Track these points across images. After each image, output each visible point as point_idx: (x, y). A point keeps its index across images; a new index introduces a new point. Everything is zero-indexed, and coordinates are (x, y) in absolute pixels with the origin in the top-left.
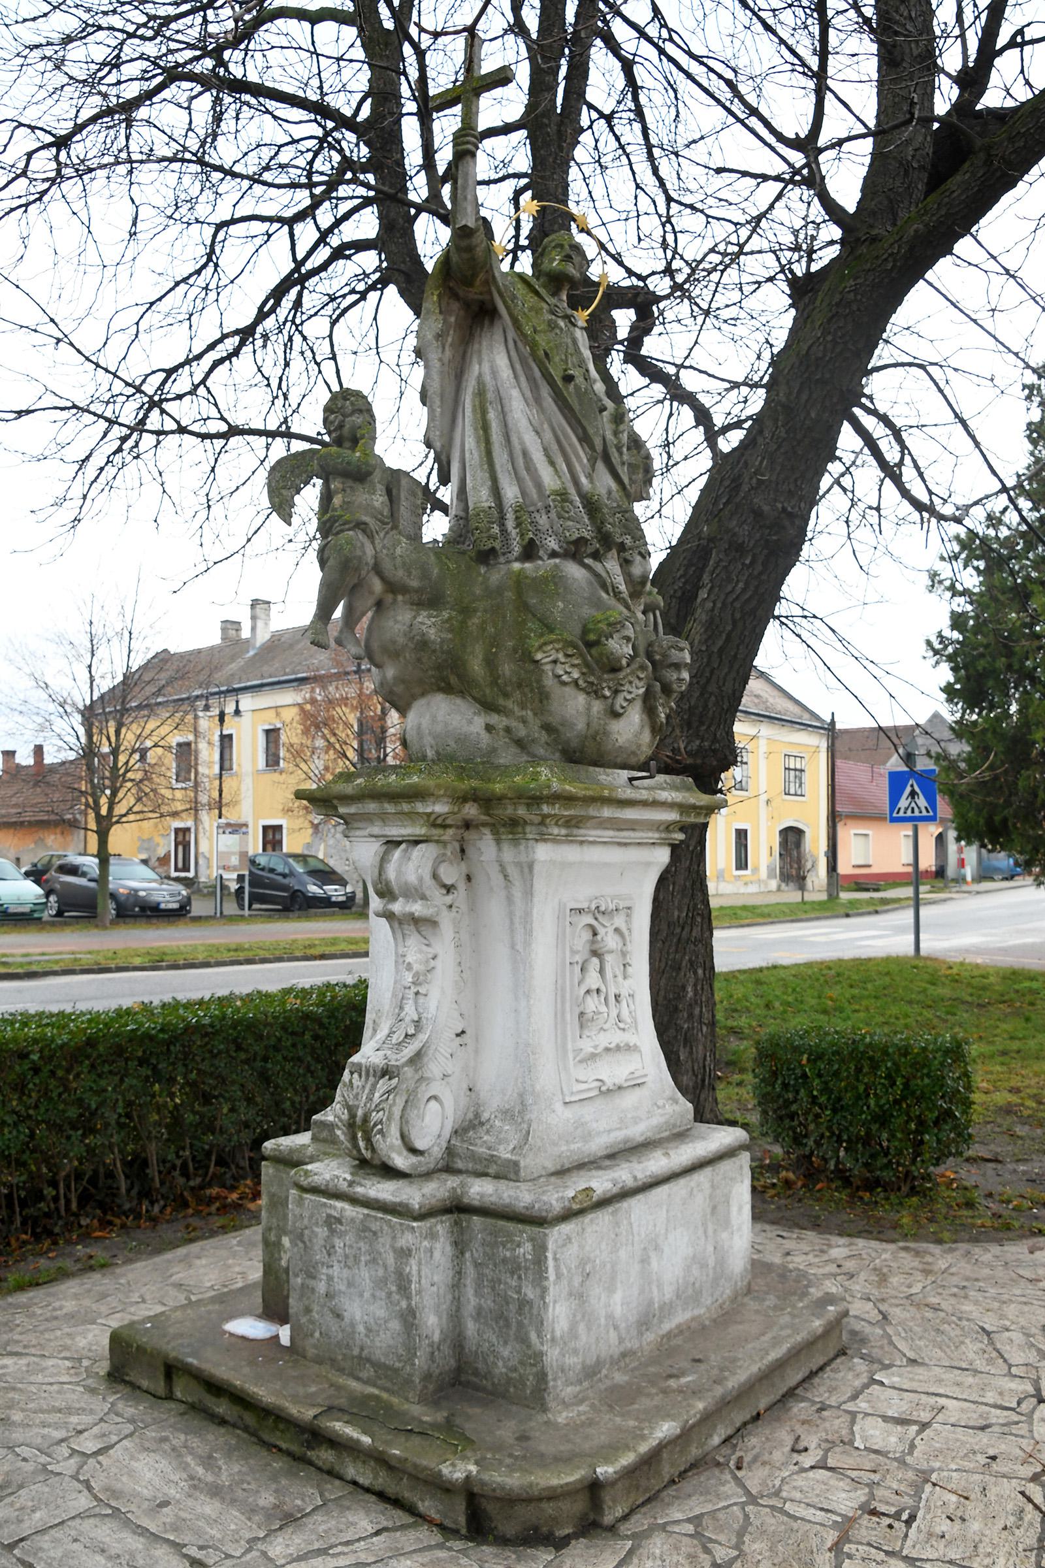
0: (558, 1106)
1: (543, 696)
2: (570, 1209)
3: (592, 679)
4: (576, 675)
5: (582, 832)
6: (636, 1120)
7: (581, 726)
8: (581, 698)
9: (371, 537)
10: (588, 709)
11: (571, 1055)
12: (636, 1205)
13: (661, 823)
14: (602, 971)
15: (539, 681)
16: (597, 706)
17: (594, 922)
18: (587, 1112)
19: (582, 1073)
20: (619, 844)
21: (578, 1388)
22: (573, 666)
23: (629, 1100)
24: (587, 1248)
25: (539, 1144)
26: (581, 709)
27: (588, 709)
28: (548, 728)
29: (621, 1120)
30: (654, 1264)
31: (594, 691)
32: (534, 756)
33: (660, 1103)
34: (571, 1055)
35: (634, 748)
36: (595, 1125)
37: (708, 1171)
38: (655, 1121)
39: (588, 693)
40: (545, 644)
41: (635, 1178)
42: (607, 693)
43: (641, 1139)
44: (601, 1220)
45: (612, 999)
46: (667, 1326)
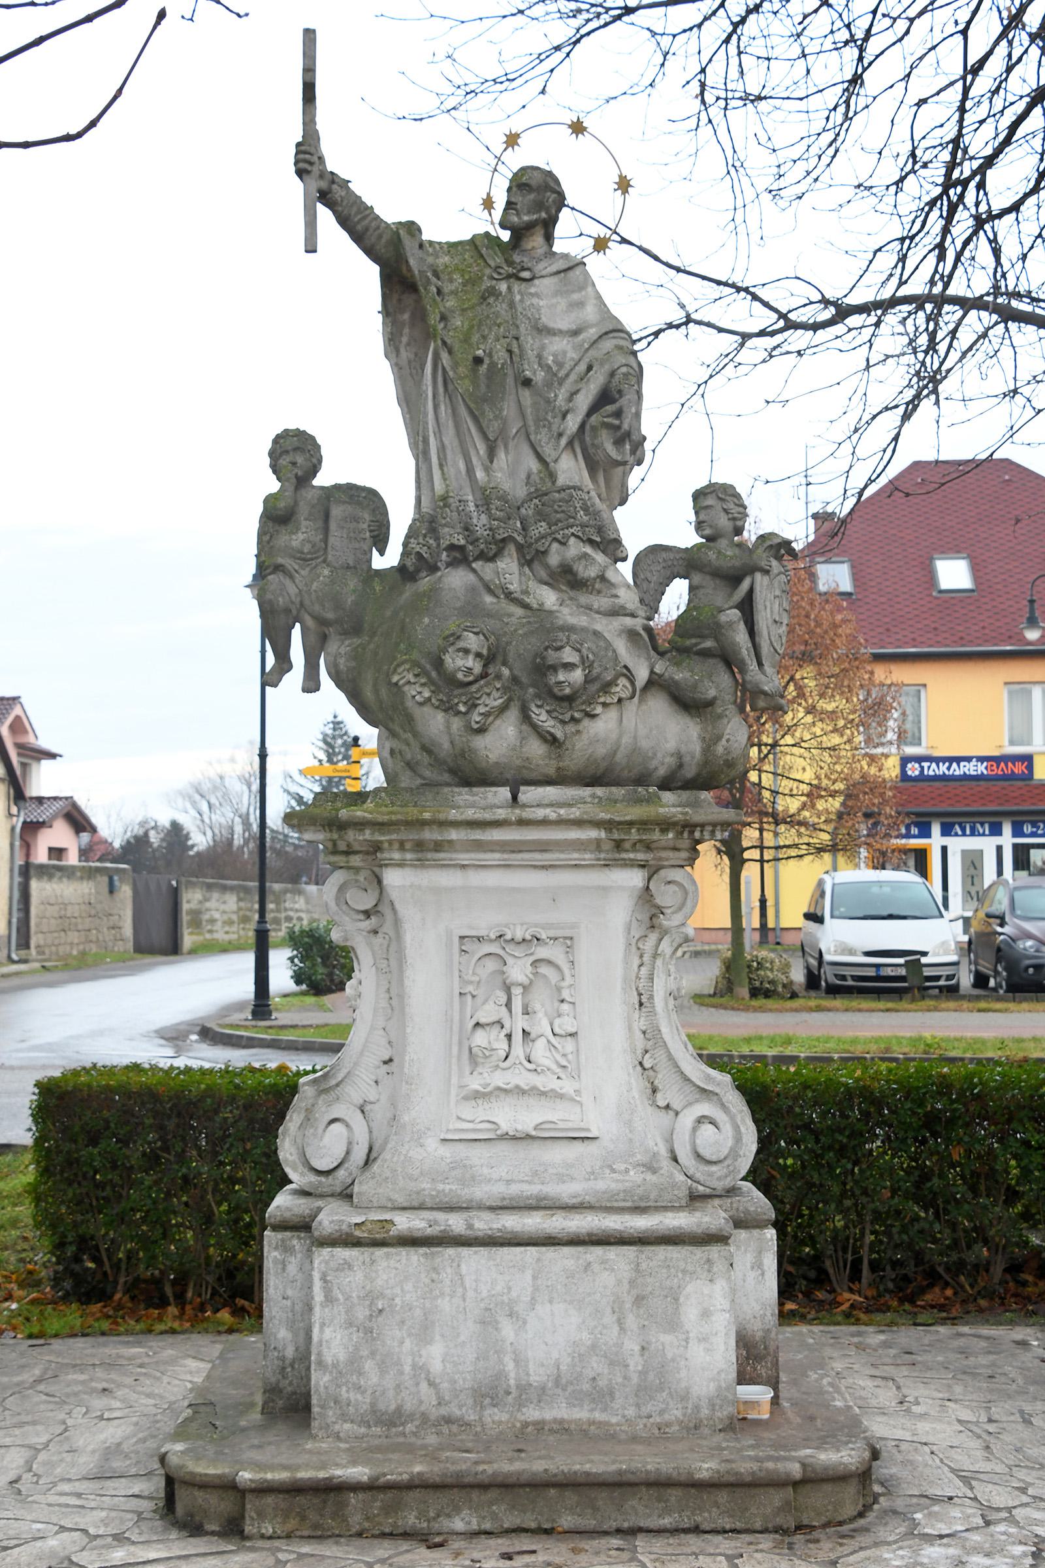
0: (432, 1144)
1: (409, 719)
2: (351, 1235)
3: (441, 696)
4: (427, 694)
5: (442, 855)
6: (561, 1179)
7: (446, 745)
8: (440, 716)
9: (291, 577)
10: (448, 727)
11: (454, 1091)
12: (473, 1260)
13: (590, 841)
14: (508, 1005)
15: (402, 703)
16: (457, 723)
17: (501, 952)
18: (478, 1156)
19: (468, 1111)
20: (535, 867)
21: (363, 1430)
22: (423, 685)
24: (379, 1282)
25: (388, 1174)
26: (441, 727)
27: (448, 727)
28: (424, 748)
29: (536, 1173)
30: (508, 1330)
31: (448, 708)
32: (424, 779)
34: (454, 1091)
35: (518, 762)
36: (486, 1171)
37: (630, 1251)
38: (601, 1185)
39: (445, 711)
40: (398, 666)
41: (470, 1227)
42: (462, 708)
45: (518, 1037)
46: (532, 1413)
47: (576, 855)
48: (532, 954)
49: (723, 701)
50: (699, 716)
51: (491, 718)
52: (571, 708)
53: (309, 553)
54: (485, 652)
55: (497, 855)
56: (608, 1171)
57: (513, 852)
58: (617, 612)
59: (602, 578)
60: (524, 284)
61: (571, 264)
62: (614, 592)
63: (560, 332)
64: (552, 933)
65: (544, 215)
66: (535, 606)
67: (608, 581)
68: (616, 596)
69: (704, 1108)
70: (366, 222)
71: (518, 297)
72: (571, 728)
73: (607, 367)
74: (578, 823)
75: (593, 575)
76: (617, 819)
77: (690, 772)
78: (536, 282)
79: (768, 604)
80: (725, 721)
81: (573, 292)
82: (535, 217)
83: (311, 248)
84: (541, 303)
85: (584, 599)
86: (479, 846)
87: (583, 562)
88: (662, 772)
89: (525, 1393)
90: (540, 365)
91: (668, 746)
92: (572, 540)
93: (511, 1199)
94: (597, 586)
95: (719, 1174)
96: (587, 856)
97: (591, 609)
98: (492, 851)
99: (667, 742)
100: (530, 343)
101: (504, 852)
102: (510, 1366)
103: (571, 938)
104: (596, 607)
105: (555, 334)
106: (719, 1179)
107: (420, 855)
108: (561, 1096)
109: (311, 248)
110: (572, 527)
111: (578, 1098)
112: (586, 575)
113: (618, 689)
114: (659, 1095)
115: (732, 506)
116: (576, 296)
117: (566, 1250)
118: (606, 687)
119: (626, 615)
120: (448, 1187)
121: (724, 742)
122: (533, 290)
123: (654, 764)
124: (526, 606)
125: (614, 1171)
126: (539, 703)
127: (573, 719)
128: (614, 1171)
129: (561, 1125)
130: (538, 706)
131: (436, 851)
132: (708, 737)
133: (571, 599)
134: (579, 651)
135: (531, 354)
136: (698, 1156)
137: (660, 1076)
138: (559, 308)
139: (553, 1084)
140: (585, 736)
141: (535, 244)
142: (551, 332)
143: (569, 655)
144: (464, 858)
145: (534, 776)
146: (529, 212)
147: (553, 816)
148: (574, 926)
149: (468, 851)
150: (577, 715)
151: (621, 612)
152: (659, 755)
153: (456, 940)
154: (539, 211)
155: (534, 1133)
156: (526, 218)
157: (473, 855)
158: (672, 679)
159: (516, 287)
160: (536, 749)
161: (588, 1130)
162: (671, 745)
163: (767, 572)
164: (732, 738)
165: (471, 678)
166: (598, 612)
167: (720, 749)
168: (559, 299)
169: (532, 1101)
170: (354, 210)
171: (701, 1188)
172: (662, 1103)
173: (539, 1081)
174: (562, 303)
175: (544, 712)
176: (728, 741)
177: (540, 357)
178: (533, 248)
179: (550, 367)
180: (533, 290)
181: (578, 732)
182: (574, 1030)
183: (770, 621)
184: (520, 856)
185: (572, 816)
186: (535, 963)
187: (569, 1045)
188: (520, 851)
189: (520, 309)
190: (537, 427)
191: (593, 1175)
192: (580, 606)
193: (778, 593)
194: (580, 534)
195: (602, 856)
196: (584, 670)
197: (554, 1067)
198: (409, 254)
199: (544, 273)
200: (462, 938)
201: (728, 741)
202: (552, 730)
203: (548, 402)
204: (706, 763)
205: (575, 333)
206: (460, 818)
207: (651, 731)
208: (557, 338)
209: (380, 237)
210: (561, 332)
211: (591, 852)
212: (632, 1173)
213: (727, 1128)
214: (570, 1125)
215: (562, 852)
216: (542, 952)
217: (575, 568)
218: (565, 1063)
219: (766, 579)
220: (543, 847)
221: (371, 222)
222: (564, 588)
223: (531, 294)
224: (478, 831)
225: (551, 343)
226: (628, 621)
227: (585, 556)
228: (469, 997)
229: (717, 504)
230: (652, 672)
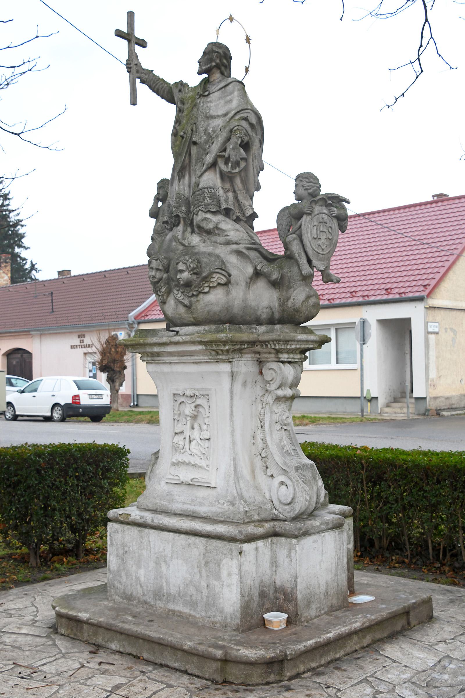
0: (163, 483)
2: (118, 518)
5: (159, 358)
6: (201, 504)
12: (153, 534)
18: (176, 490)
20: (193, 363)
21: (121, 600)
23: (202, 493)
24: (126, 540)
25: (148, 495)
29: (193, 501)
30: (164, 568)
33: (222, 501)
36: (177, 497)
37: (204, 540)
38: (214, 509)
41: (153, 521)
43: (204, 515)
44: (134, 531)
46: (171, 606)
47: (202, 357)
48: (194, 402)
49: (294, 280)
50: (279, 289)
51: (165, 297)
52: (191, 291)
53: (160, 231)
54: (161, 268)
55: (176, 358)
56: (217, 503)
57: (182, 356)
58: (228, 243)
59: (217, 228)
60: (206, 98)
61: (227, 83)
62: (226, 233)
63: (219, 116)
64: (201, 393)
65: (214, 64)
66: (187, 245)
67: (221, 229)
68: (228, 236)
69: (283, 478)
70: (157, 87)
71: (202, 104)
72: (193, 299)
73: (228, 129)
74: (193, 343)
75: (211, 227)
76: (203, 340)
77: (277, 316)
78: (211, 95)
79: (309, 230)
80: (292, 290)
81: (228, 96)
82: (208, 66)
83: (134, 102)
84: (212, 105)
85: (213, 239)
86: (171, 354)
87: (205, 222)
88: (264, 316)
89: (170, 598)
90: (205, 134)
91: (263, 304)
92: (200, 212)
93: (184, 511)
94: (216, 232)
95: (288, 510)
96: (206, 358)
97: (217, 243)
98: (175, 356)
99: (263, 302)
100: (202, 125)
101: (178, 356)
102: (164, 584)
103: (208, 395)
104: (218, 242)
105: (215, 118)
106: (288, 512)
107: (152, 358)
108: (201, 467)
109: (134, 102)
110: (200, 206)
111: (207, 469)
112: (208, 227)
113: (215, 279)
114: (268, 470)
115: (305, 183)
116: (228, 98)
117: (183, 536)
118: (206, 279)
119: (233, 244)
120: (165, 503)
121: (291, 300)
122: (209, 100)
123: (259, 313)
124: (184, 245)
125: (219, 503)
126: (177, 289)
127: (193, 295)
128: (219, 503)
129: (200, 480)
130: (177, 290)
131: (158, 356)
132: (282, 298)
133: (208, 239)
134: (185, 264)
135: (201, 130)
136: (280, 502)
137: (269, 461)
138: (220, 105)
139: (198, 461)
140: (201, 302)
141: (215, 78)
142: (213, 117)
143: (181, 267)
144: (167, 359)
145: (186, 322)
146: (205, 65)
147: (181, 340)
148: (210, 390)
149: (168, 356)
150: (194, 293)
151: (231, 243)
152: (260, 308)
153: (172, 395)
154: (211, 62)
155: (191, 483)
156: (204, 68)
157: (168, 358)
158: (263, 271)
159: (203, 99)
160: (182, 310)
161: (210, 483)
162: (265, 302)
163: (309, 214)
164: (296, 298)
165: (156, 280)
166: (220, 244)
167: (290, 304)
168: (221, 101)
169: (191, 468)
170: (152, 82)
171: (281, 516)
172: (269, 474)
173: (193, 460)
174: (222, 102)
175: (180, 292)
176: (293, 299)
177: (206, 130)
178: (214, 80)
179: (209, 134)
180: (209, 100)
181: (198, 301)
182: (208, 437)
183: (310, 238)
184: (192, 358)
185: (187, 340)
186: (196, 407)
187: (207, 443)
188: (184, 356)
189: (200, 109)
190: (196, 162)
191: (211, 504)
192: (212, 242)
193: (316, 223)
194: (203, 209)
195: (211, 357)
196: (189, 272)
197: (199, 454)
198: (175, 96)
199: (214, 91)
200: (174, 394)
201: (293, 299)
202: (183, 301)
203: (205, 150)
204: (284, 311)
205: (225, 115)
206: (152, 342)
207: (256, 296)
208: (216, 119)
209: (164, 91)
210: (218, 116)
211: (208, 356)
212: (225, 505)
213: (291, 488)
214: (203, 480)
215: (197, 356)
216: (199, 402)
217: (201, 225)
218: (204, 452)
219: (309, 218)
220: (192, 354)
221: (159, 86)
222: (204, 235)
223: (208, 102)
224: (163, 348)
225: (213, 122)
226: (235, 247)
227: (205, 219)
228: (176, 421)
229: (307, 184)
230: (255, 269)
